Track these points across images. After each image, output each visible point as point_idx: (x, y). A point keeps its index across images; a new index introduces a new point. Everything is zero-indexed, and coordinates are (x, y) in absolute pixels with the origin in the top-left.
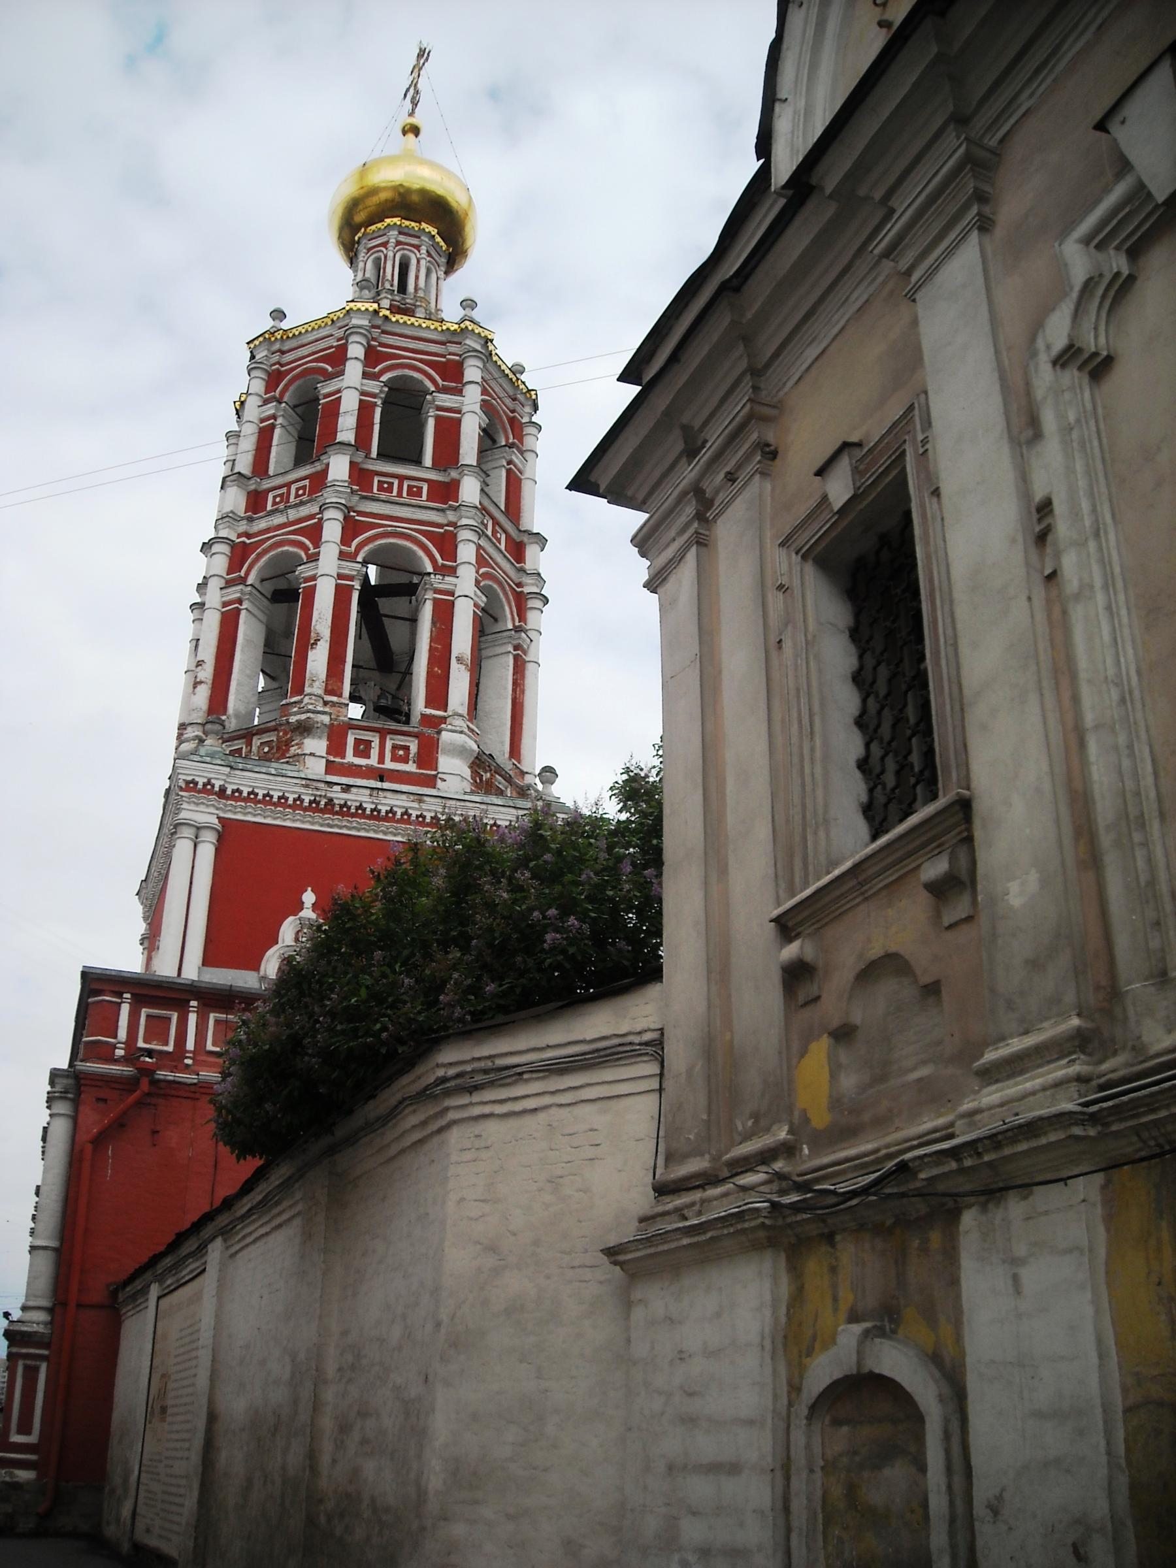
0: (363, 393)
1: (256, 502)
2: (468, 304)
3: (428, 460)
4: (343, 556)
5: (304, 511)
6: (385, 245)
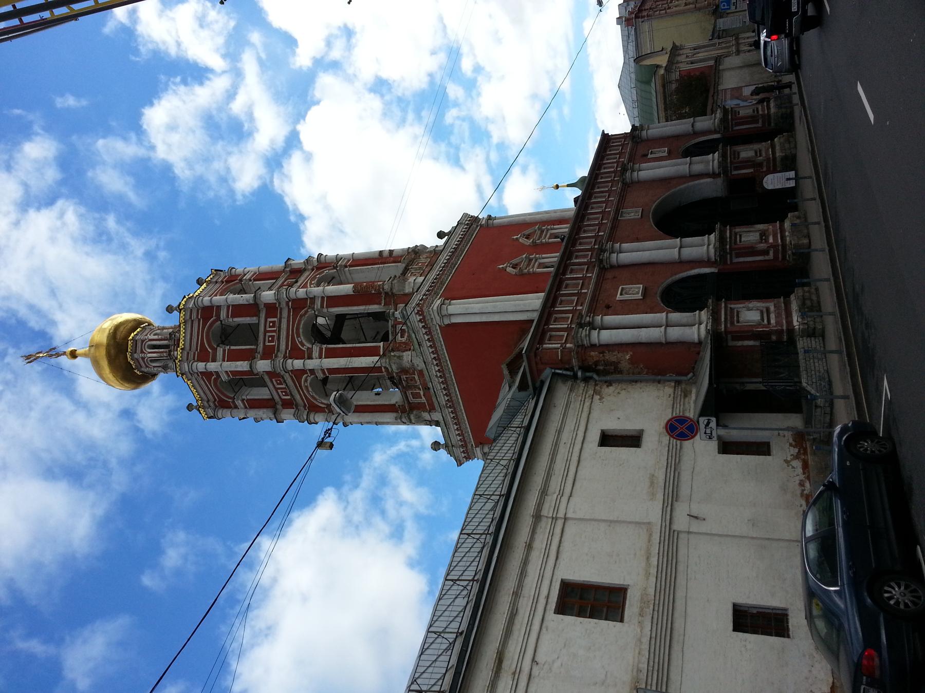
1: (288, 404)
3: (254, 320)
4: (310, 358)
5: (289, 381)
6: (143, 359)
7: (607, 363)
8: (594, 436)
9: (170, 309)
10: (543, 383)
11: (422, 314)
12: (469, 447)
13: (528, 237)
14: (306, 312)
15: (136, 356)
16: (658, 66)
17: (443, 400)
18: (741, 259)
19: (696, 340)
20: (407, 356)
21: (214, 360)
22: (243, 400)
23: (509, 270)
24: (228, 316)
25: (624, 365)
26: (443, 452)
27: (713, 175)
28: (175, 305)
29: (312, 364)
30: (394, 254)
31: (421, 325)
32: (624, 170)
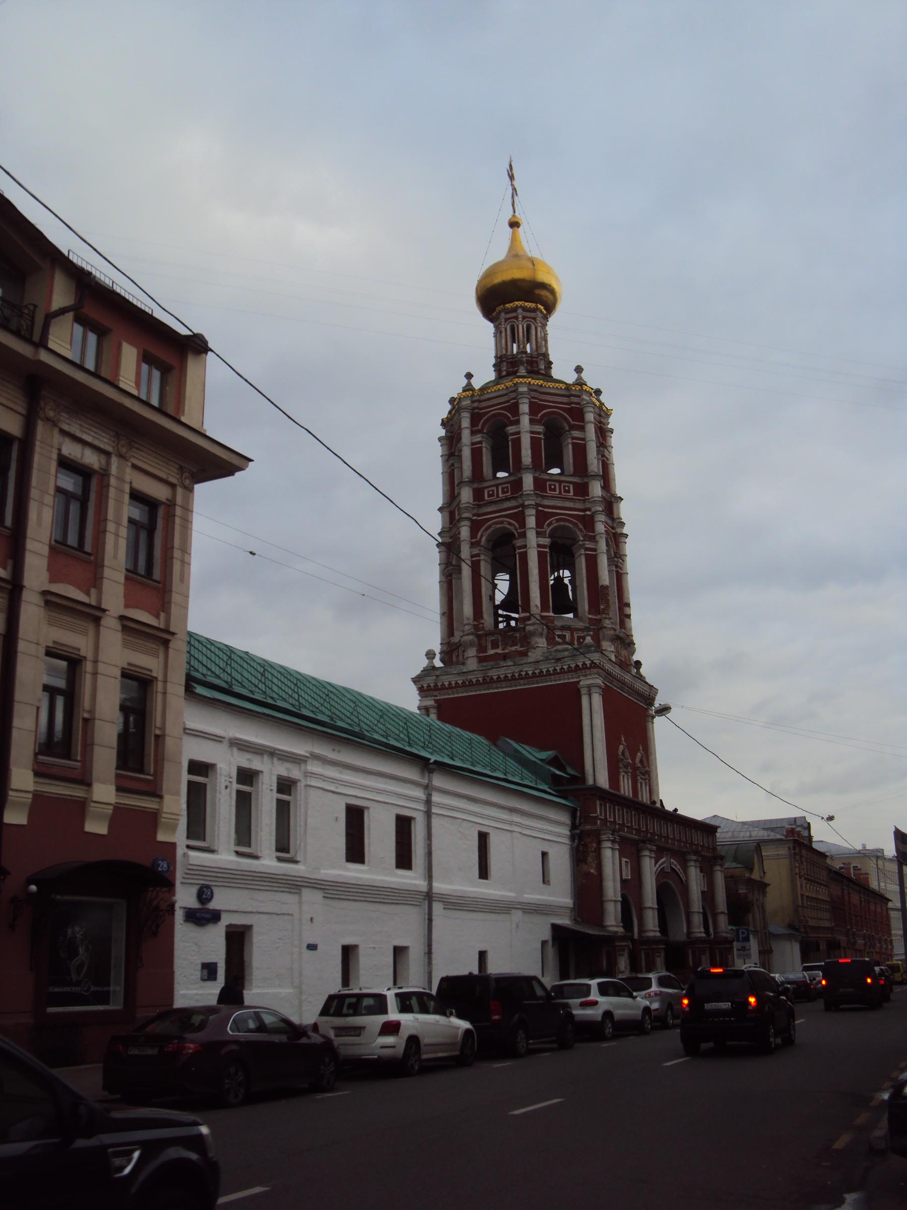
0: (532, 432)
1: (478, 495)
2: (579, 370)
6: (516, 318)
8: (546, 847)
9: (579, 370)
10: (565, 798)
11: (591, 667)
12: (435, 693)
13: (641, 761)
14: (581, 530)
15: (520, 311)
16: (751, 870)
17: (494, 673)
18: (643, 957)
19: (605, 924)
20: (542, 642)
21: (532, 421)
22: (480, 442)
23: (621, 747)
24: (573, 438)
26: (425, 662)
27: (689, 932)
28: (583, 375)
29: (531, 536)
31: (580, 664)
32: (696, 853)
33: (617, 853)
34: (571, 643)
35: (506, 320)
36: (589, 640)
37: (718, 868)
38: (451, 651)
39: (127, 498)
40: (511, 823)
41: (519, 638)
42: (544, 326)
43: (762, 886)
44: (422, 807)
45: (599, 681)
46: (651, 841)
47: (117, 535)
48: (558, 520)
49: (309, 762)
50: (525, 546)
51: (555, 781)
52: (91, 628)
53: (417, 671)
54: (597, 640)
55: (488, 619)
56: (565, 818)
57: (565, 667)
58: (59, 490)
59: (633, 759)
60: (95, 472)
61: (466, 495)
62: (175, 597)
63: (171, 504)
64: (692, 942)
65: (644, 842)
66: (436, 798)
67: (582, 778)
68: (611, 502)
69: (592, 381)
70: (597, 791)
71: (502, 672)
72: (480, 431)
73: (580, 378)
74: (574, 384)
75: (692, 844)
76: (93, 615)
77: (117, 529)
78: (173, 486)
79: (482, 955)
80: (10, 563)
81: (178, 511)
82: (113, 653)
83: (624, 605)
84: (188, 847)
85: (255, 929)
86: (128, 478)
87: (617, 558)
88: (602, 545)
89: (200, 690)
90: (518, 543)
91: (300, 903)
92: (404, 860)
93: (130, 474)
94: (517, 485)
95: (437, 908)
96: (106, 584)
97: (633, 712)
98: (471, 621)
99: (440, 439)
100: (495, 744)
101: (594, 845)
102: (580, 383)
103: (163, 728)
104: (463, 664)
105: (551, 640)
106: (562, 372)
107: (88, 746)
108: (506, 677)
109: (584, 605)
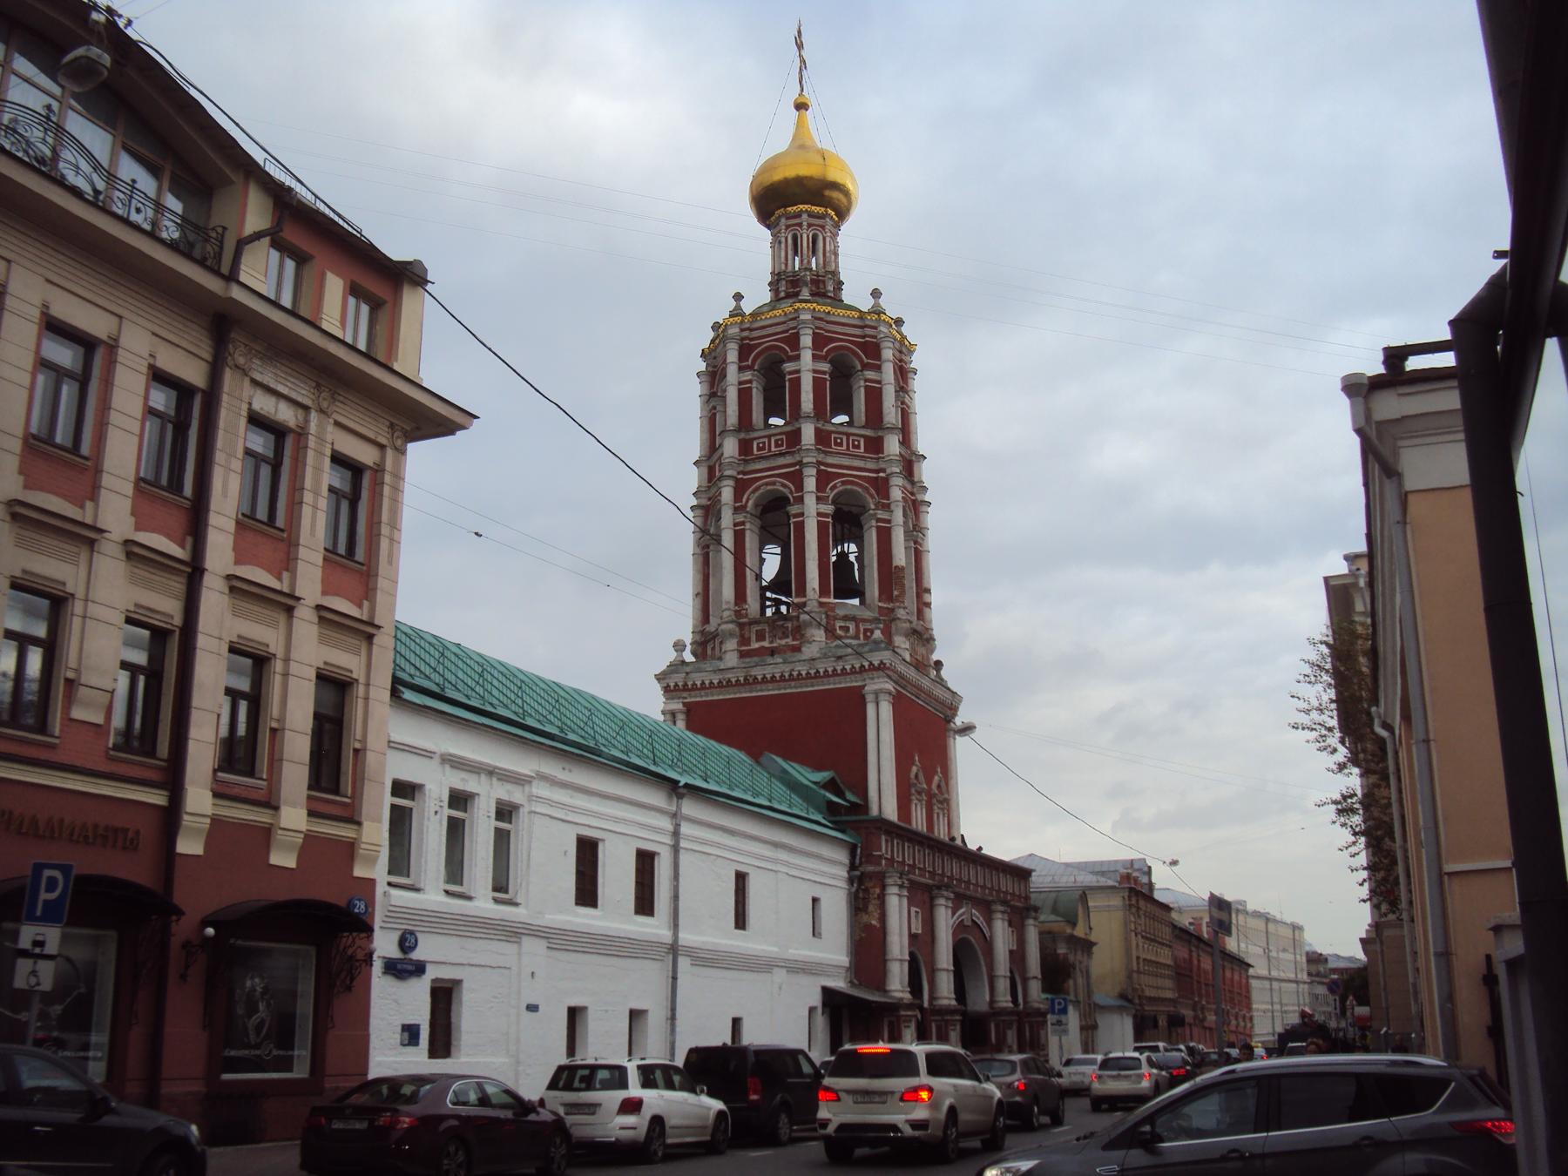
0: (815, 371)
1: (745, 447)
2: (876, 294)
4: (819, 499)
6: (800, 225)
7: (866, 901)
9: (876, 294)
10: (843, 831)
13: (939, 786)
15: (805, 216)
16: (1074, 924)
17: (758, 672)
20: (819, 635)
22: (750, 382)
23: (914, 769)
24: (866, 380)
25: (865, 918)
26: (672, 656)
27: (992, 1001)
30: (926, 610)
32: (1004, 902)
33: (905, 901)
34: (856, 637)
35: (787, 227)
36: (878, 634)
37: (1031, 921)
38: (705, 643)
39: (327, 461)
40: (775, 861)
41: (790, 628)
42: (835, 235)
43: (1087, 946)
44: (668, 840)
45: (890, 686)
46: (947, 887)
47: (315, 507)
48: (843, 483)
49: (535, 783)
50: (802, 514)
51: (831, 809)
52: (282, 618)
53: (662, 667)
54: (888, 633)
55: (753, 604)
56: (842, 856)
57: (848, 667)
58: (248, 452)
59: (929, 782)
60: (291, 430)
61: (730, 447)
62: (382, 583)
63: (379, 470)
64: (995, 1013)
65: (939, 888)
66: (686, 829)
67: (864, 807)
68: (910, 462)
69: (892, 310)
70: (882, 825)
71: (768, 671)
72: (750, 368)
73: (877, 305)
74: (869, 313)
75: (999, 891)
76: (286, 604)
77: (316, 500)
78: (382, 447)
79: (736, 1022)
80: (189, 540)
81: (387, 478)
82: (306, 651)
83: (922, 590)
84: (389, 884)
85: (465, 985)
86: (329, 438)
87: (916, 532)
88: (898, 516)
89: (408, 695)
90: (793, 509)
91: (519, 954)
92: (645, 905)
93: (332, 434)
94: (794, 437)
95: (683, 963)
96: (301, 566)
97: (930, 728)
98: (732, 605)
99: (698, 375)
100: (757, 762)
101: (878, 891)
102: (877, 311)
103: (364, 741)
104: (720, 659)
105: (830, 632)
106: (855, 294)
107: (276, 761)
108: (773, 677)
109: (873, 589)
